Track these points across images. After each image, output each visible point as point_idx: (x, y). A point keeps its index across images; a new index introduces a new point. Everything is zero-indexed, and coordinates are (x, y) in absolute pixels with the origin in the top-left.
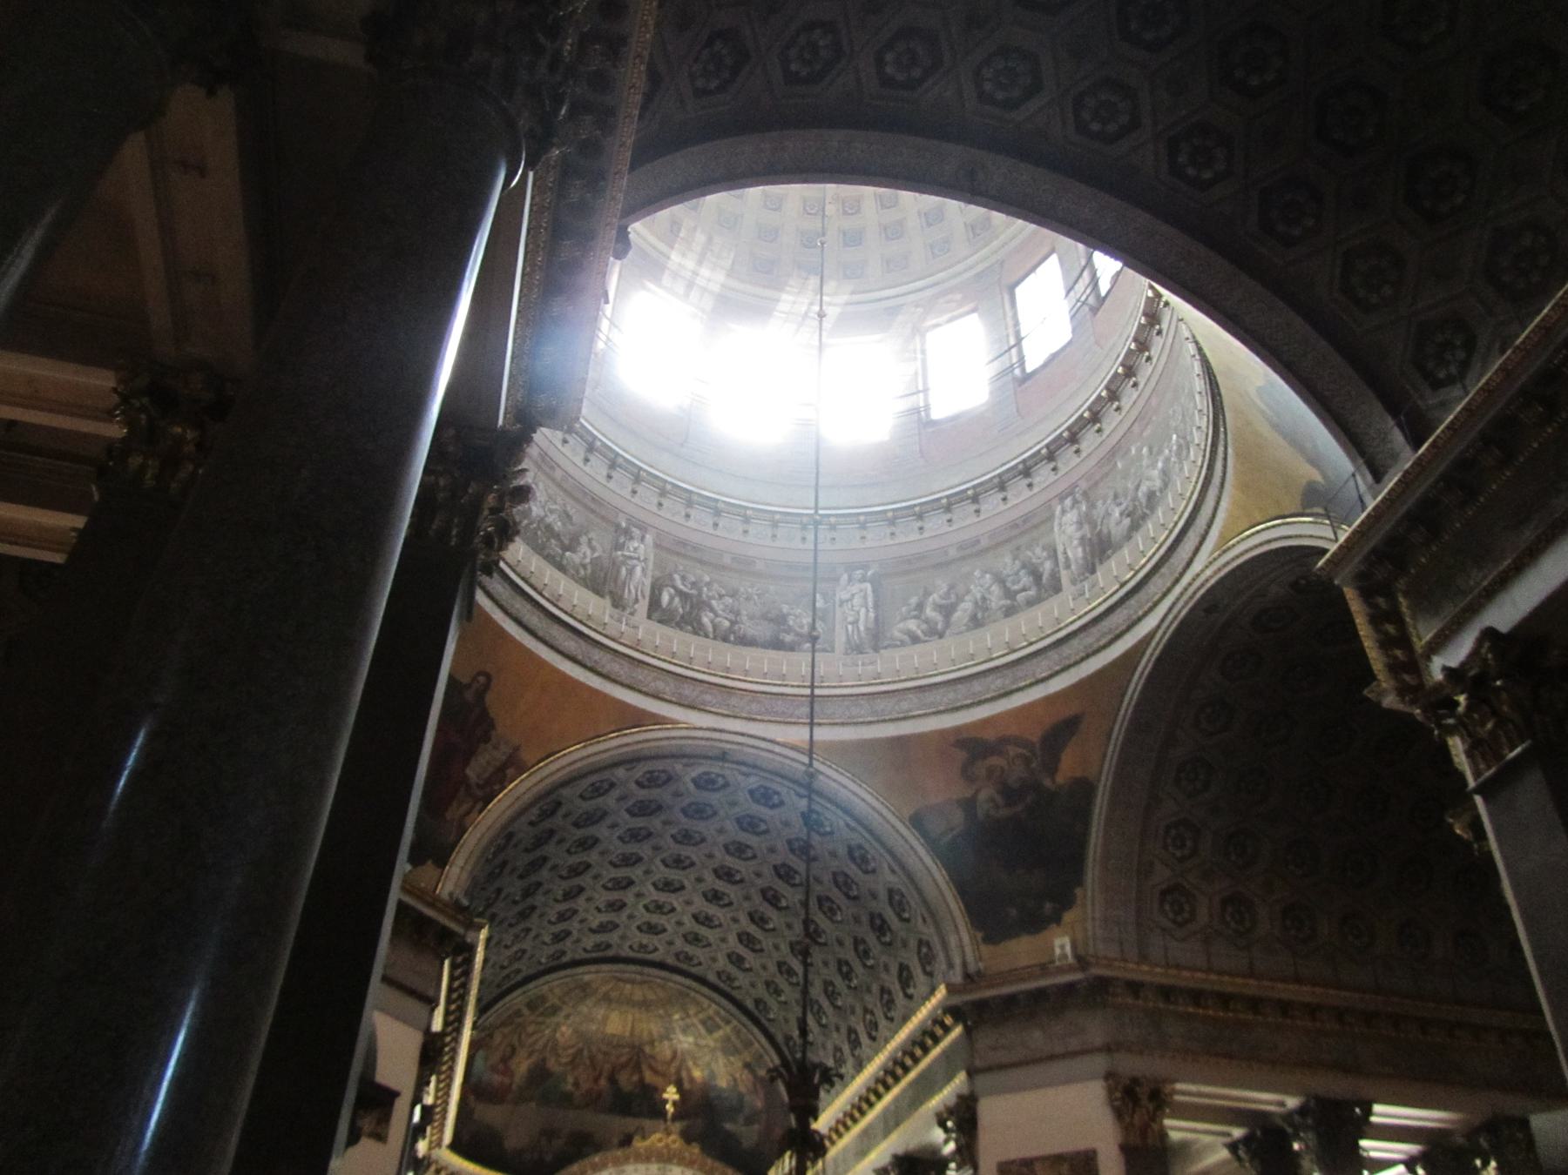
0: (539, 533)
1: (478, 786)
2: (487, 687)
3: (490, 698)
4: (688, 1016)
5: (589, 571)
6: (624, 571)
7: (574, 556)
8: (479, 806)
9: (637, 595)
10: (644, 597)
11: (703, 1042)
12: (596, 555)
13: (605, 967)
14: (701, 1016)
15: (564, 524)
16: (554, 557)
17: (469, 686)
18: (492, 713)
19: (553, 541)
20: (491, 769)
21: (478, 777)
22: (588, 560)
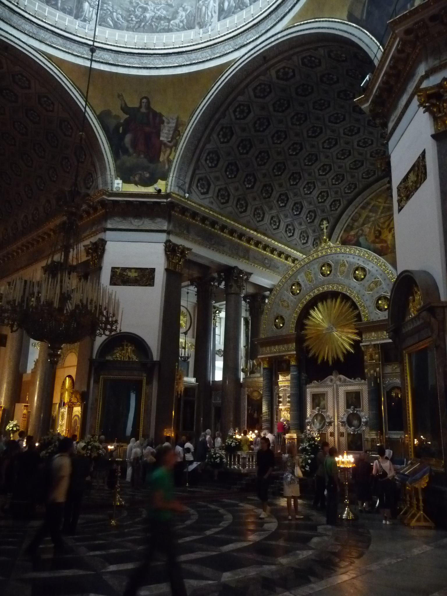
0: (153, 23)
1: (170, 142)
2: (148, 102)
3: (152, 107)
5: (185, 21)
6: (204, 8)
7: (175, 21)
8: (173, 149)
9: (212, 15)
10: (215, 12)
12: (188, 11)
15: (167, 11)
16: (164, 29)
17: (141, 107)
18: (158, 111)
19: (162, 22)
20: (171, 132)
21: (167, 138)
22: (184, 17)
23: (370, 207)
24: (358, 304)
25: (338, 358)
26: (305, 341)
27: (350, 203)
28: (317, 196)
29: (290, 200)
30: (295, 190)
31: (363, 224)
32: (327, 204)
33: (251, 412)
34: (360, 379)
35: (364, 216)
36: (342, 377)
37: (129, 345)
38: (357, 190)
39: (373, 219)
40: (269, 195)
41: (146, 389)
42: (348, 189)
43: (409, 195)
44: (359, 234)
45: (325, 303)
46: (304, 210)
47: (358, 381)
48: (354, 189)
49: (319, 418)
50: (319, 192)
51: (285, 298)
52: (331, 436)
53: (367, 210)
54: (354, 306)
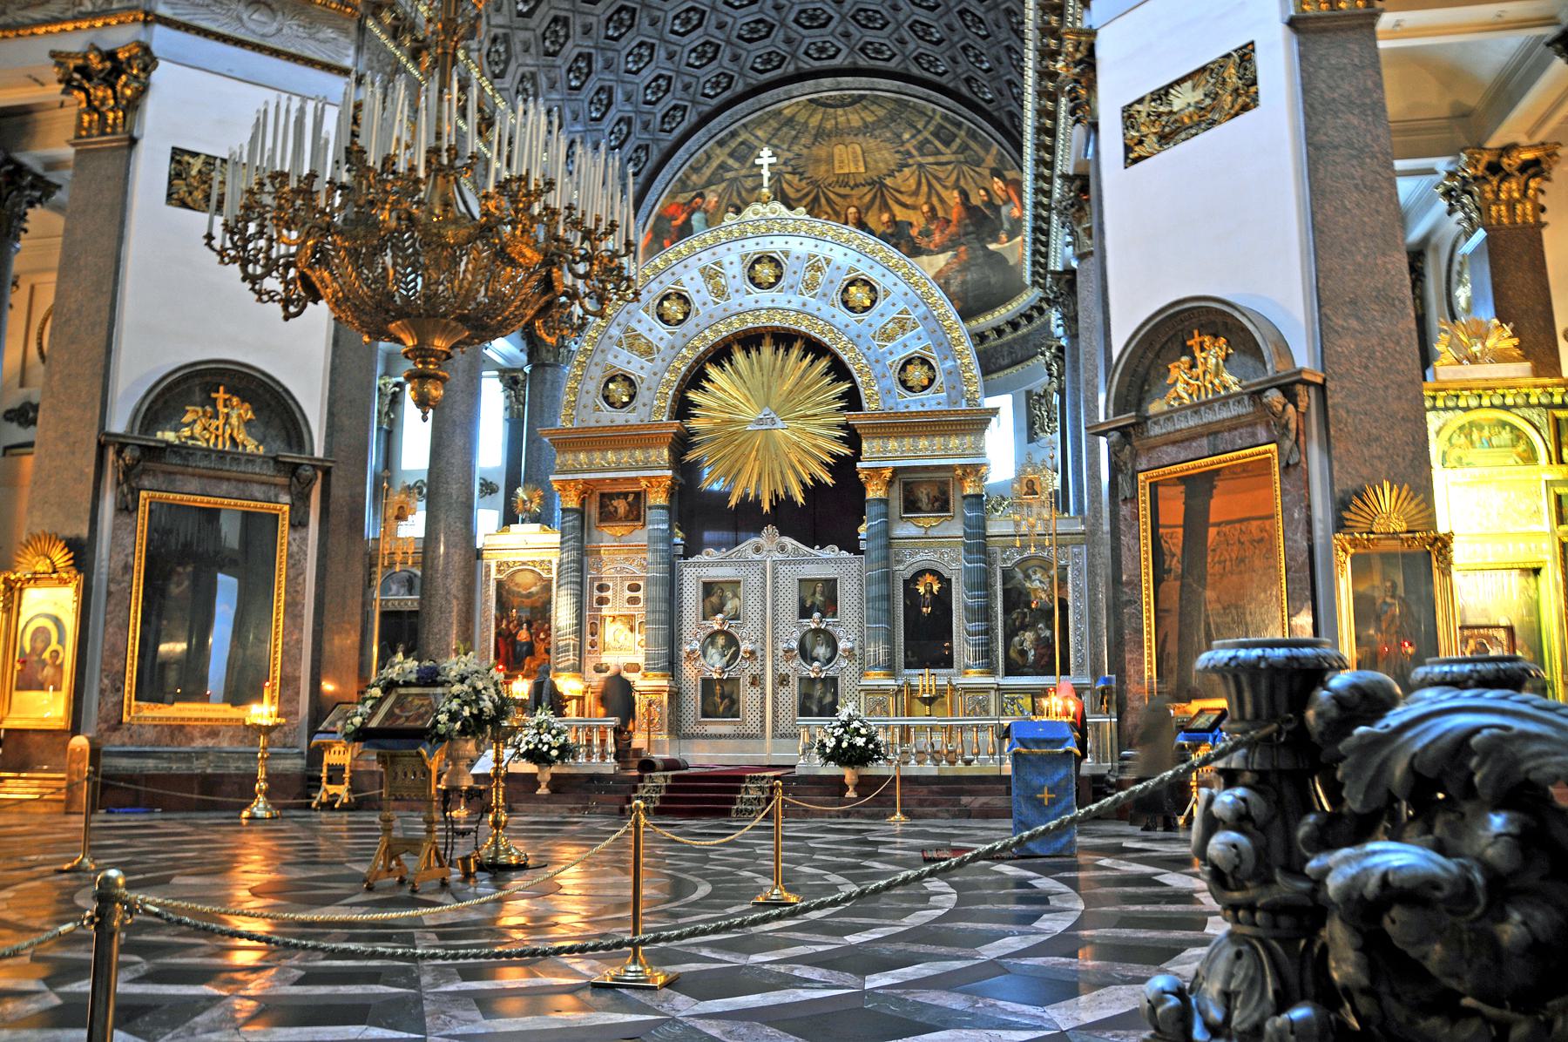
4: (919, 132)
11: (943, 159)
13: (795, 88)
14: (931, 128)
23: (733, 144)
24: (853, 369)
25: (790, 499)
26: (690, 446)
27: (704, 120)
28: (646, 82)
29: (593, 75)
30: (610, 54)
31: (709, 183)
32: (660, 110)
33: (508, 625)
34: (836, 548)
35: (715, 164)
36: (788, 541)
37: (235, 400)
38: (727, 94)
39: (729, 175)
40: (557, 48)
41: (289, 543)
42: (712, 88)
43: (1175, 132)
44: (693, 205)
45: (753, 353)
46: (613, 110)
47: (831, 552)
48: (725, 89)
49: (721, 641)
50: (655, 74)
51: (641, 329)
52: (753, 684)
53: (727, 150)
54: (839, 370)
